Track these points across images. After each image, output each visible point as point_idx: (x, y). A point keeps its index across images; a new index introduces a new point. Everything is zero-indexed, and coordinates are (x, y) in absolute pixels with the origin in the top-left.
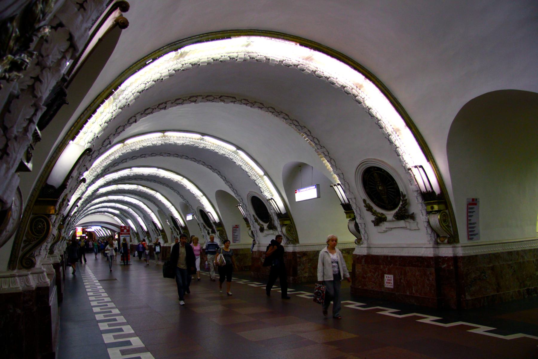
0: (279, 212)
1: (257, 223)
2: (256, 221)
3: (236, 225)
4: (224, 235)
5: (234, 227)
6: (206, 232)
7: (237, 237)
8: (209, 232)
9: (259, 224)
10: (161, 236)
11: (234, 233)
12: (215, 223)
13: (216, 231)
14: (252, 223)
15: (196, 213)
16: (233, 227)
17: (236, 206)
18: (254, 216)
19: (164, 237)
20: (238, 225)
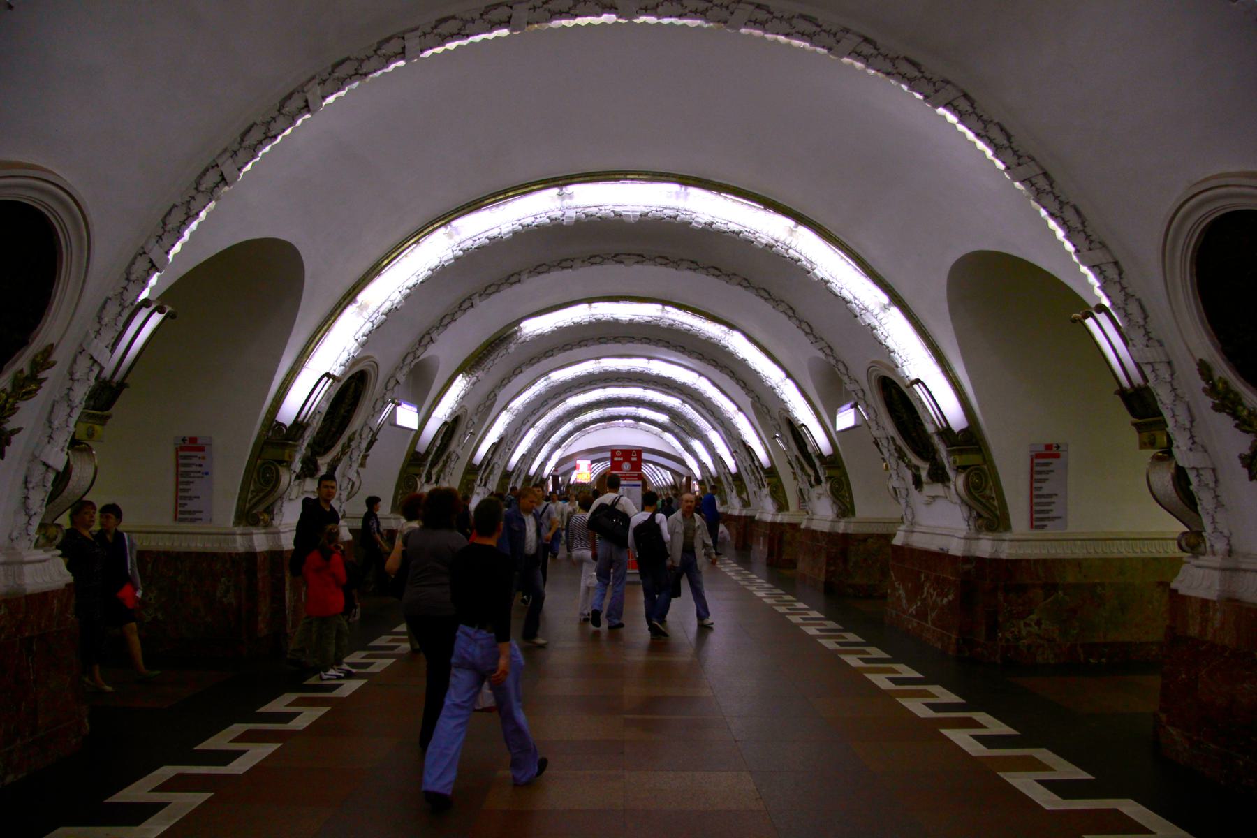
1: (1234, 415)
3: (1048, 447)
4: (988, 492)
6: (908, 474)
7: (1049, 504)
8: (920, 476)
11: (1036, 485)
13: (951, 474)
14: (1183, 419)
15: (864, 394)
17: (1074, 321)
18: (1204, 369)
19: (775, 492)
20: (1058, 447)
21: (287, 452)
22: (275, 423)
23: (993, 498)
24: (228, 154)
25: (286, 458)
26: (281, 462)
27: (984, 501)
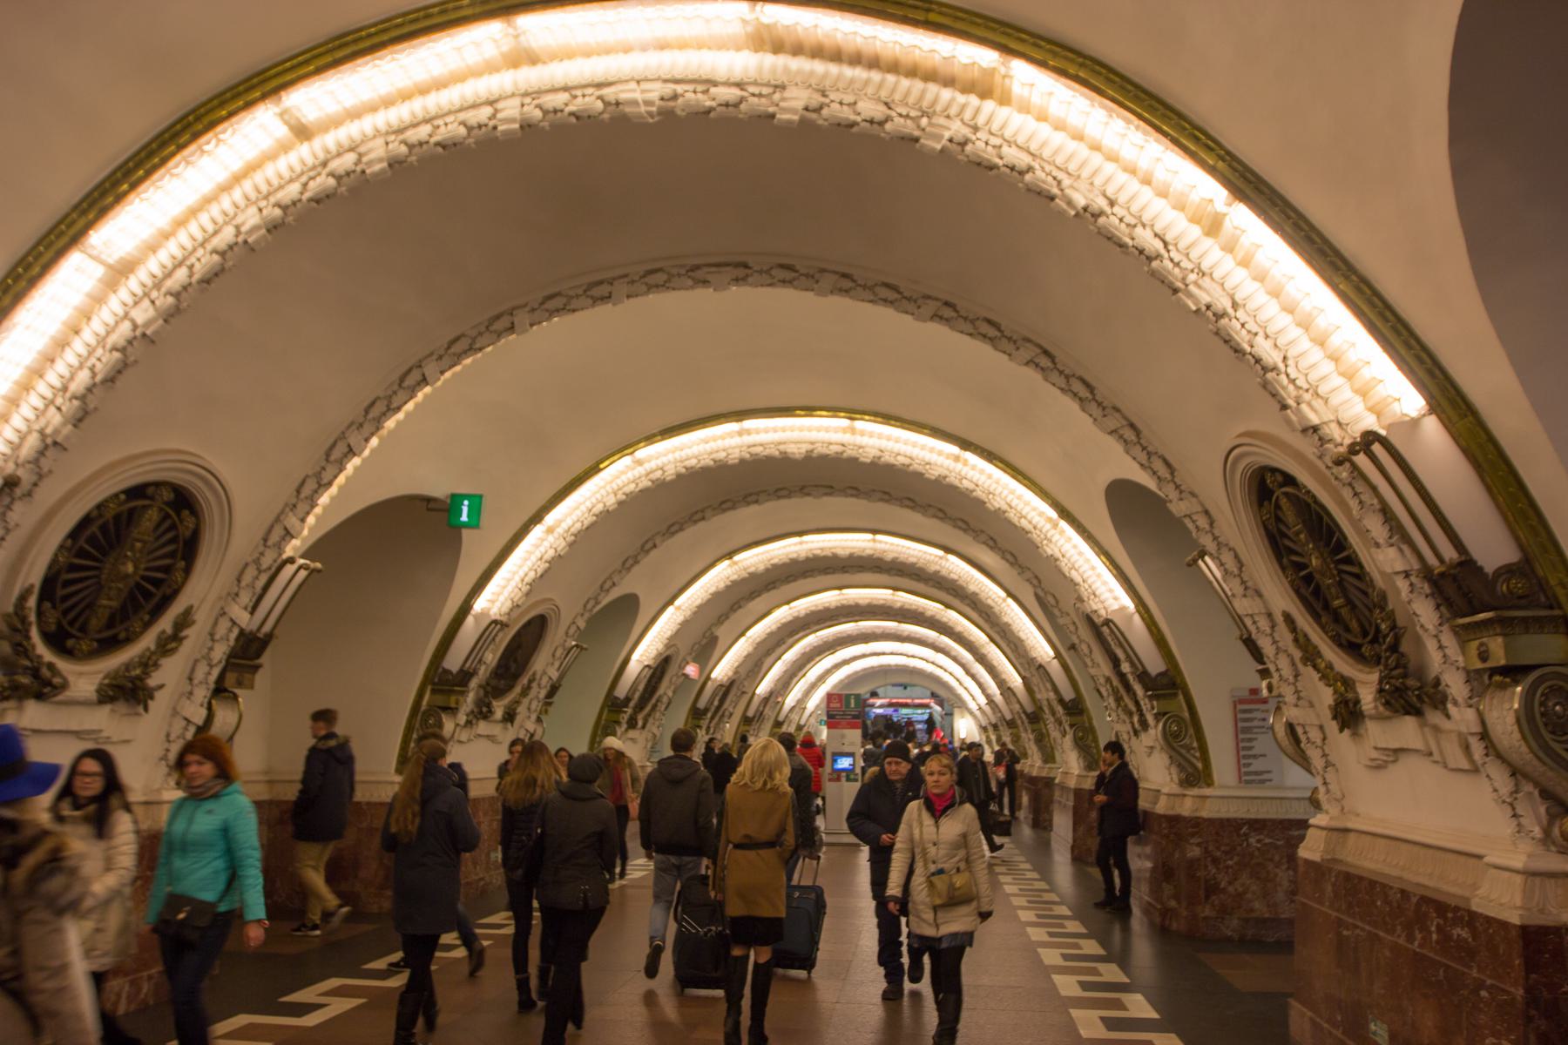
0: (1450, 553)
1: (1315, 667)
2: (1311, 655)
5: (1242, 701)
9: (1329, 675)
10: (1154, 734)
12: (1143, 676)
16: (1237, 702)
18: (1289, 620)
21: (453, 698)
22: (440, 670)
23: (1193, 749)
24: (354, 427)
25: (453, 705)
26: (446, 709)
27: (1183, 751)
